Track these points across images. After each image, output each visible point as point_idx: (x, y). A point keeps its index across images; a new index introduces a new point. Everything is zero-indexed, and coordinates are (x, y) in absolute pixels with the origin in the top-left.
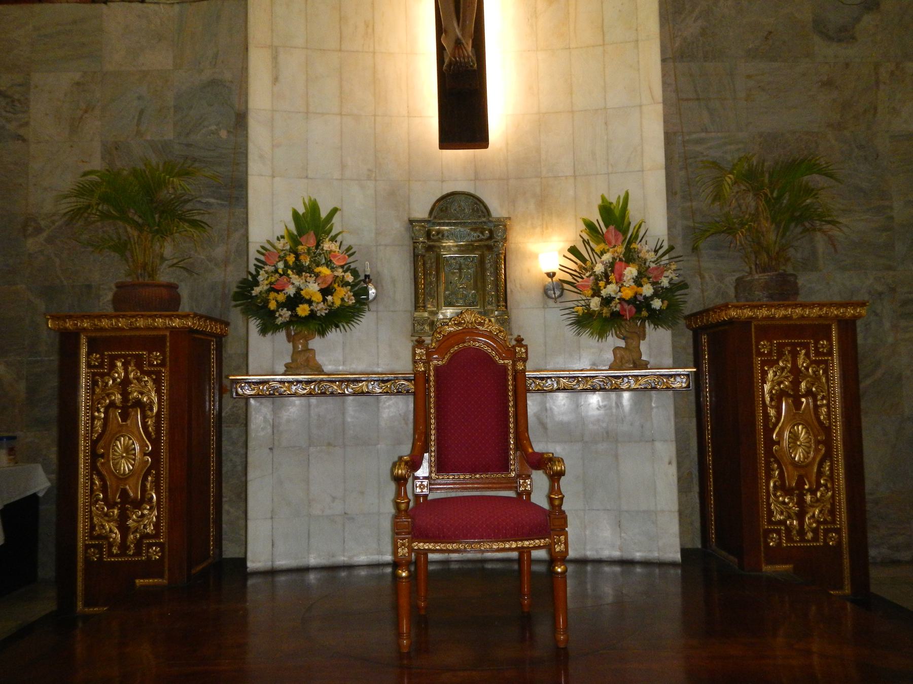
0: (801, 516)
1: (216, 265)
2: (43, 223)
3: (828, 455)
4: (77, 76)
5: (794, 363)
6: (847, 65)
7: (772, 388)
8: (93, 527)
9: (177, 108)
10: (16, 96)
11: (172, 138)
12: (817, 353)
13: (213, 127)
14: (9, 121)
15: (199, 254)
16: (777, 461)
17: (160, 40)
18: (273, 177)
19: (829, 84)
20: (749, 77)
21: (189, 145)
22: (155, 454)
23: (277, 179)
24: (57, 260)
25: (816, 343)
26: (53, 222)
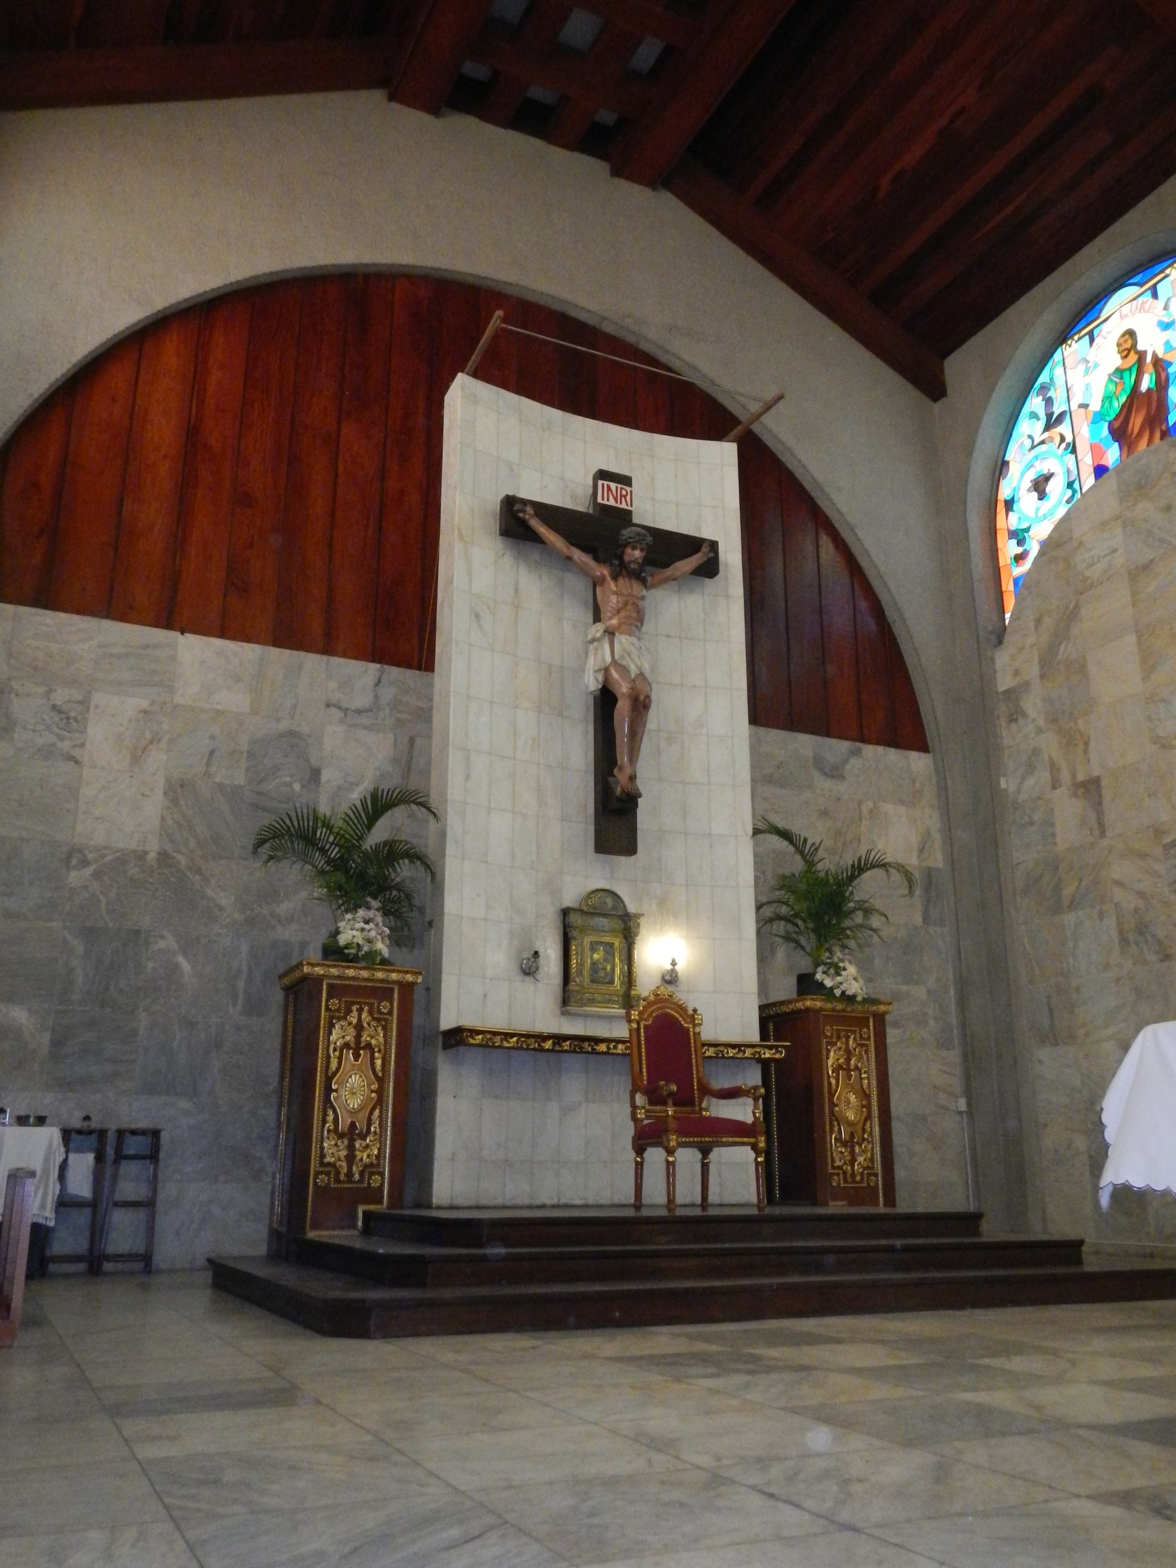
0: (852, 1161)
1: (279, 921)
2: (90, 857)
3: (869, 1117)
4: (145, 704)
5: (847, 1044)
6: (839, 799)
7: (833, 1063)
8: (323, 1156)
9: (251, 754)
10: (73, 714)
11: (242, 782)
12: (862, 1038)
13: (288, 779)
14: (62, 739)
15: (262, 908)
16: (837, 1120)
17: (238, 681)
18: (463, 859)
19: (824, 813)
20: (765, 799)
21: (260, 794)
22: (380, 1092)
23: (466, 861)
24: (102, 898)
25: (860, 1031)
26: (103, 857)
